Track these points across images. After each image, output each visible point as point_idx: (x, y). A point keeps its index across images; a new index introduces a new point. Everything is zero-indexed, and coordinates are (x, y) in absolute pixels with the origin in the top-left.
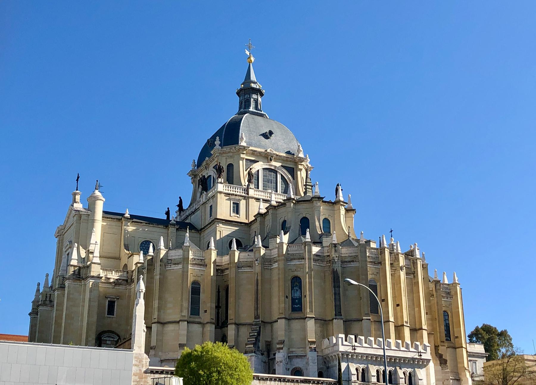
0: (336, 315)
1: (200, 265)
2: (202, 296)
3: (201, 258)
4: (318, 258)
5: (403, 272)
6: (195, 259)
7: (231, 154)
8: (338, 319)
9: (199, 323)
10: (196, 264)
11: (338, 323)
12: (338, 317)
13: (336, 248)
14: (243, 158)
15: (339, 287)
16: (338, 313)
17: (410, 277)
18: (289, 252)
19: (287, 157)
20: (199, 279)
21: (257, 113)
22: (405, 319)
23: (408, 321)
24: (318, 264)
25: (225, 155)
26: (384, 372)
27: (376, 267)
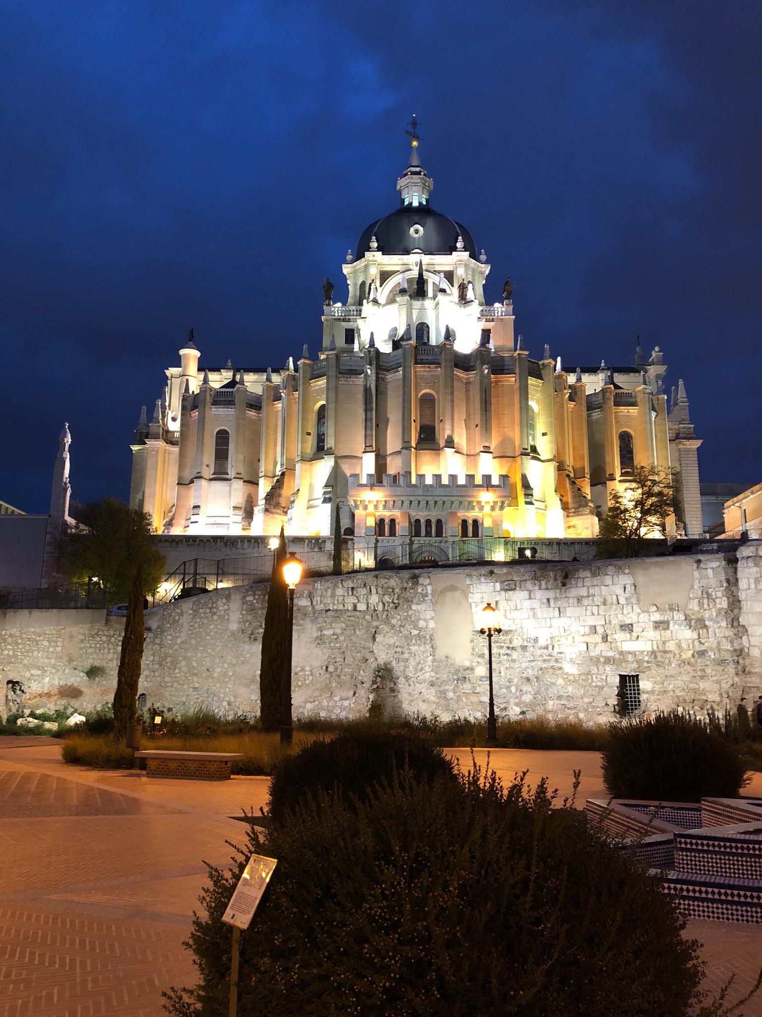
26: (428, 522)
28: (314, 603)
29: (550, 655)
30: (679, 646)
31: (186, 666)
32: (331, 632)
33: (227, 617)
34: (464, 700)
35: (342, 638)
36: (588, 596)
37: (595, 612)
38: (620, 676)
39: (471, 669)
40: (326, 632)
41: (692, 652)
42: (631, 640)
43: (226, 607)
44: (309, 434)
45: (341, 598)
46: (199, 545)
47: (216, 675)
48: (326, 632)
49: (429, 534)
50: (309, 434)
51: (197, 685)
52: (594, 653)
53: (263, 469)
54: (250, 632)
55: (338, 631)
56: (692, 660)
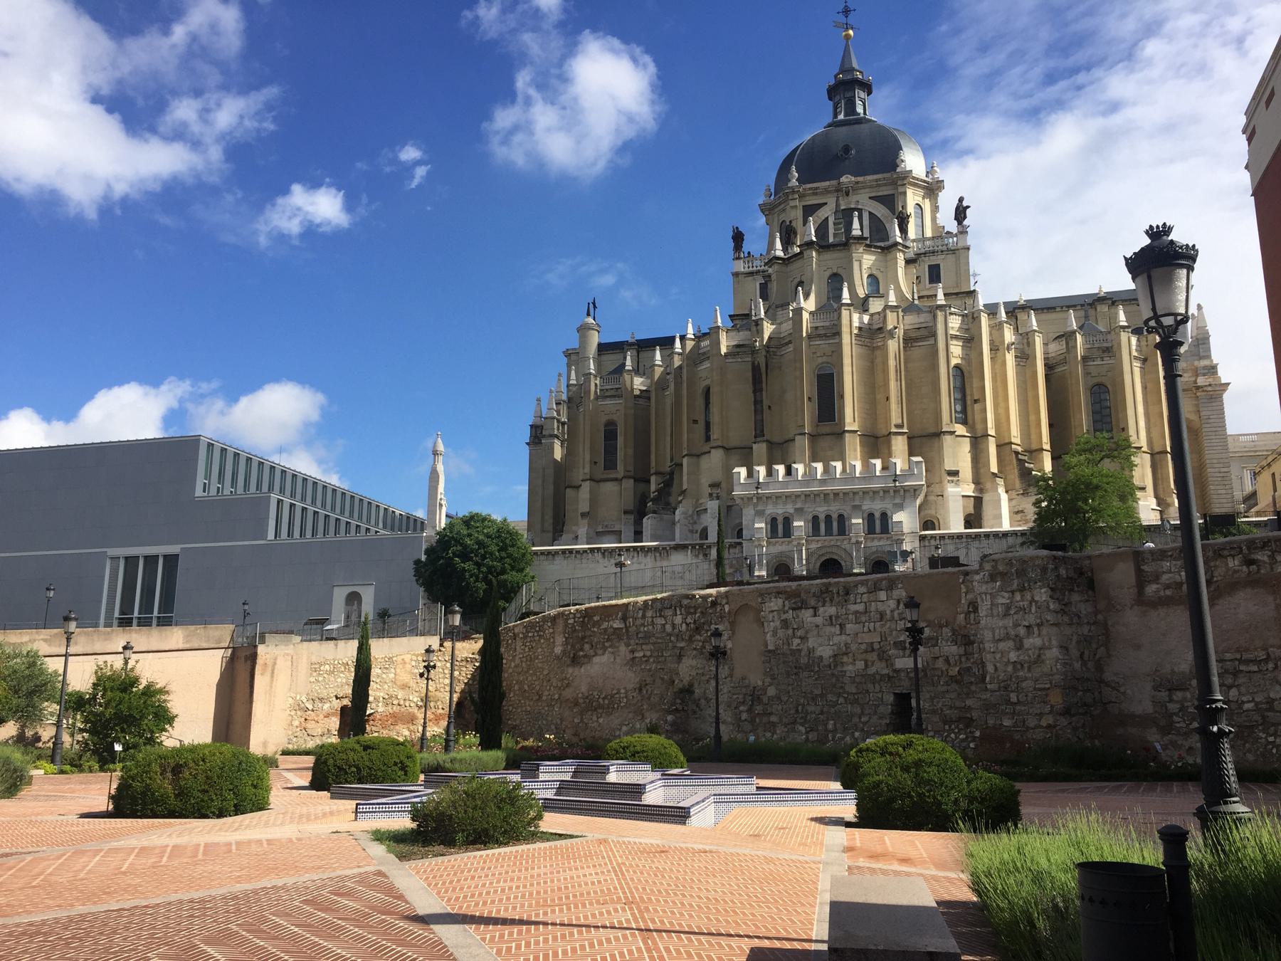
0: (755, 437)
1: (614, 396)
2: (620, 440)
3: (617, 386)
4: (738, 350)
5: (896, 339)
6: (607, 390)
7: (782, 206)
8: (758, 442)
9: (616, 479)
10: (607, 397)
11: (760, 449)
12: (758, 439)
13: (759, 327)
14: (796, 207)
15: (761, 390)
16: (759, 434)
17: (928, 343)
18: (701, 351)
19: (877, 180)
20: (615, 417)
21: (850, 120)
22: (895, 418)
23: (903, 422)
24: (739, 360)
25: (776, 210)
26: (828, 518)
27: (831, 341)
28: (628, 624)
29: (833, 674)
30: (947, 661)
31: (520, 689)
32: (641, 654)
33: (552, 640)
34: (757, 720)
35: (651, 660)
36: (866, 612)
37: (872, 629)
38: (895, 694)
39: (765, 690)
40: (637, 655)
41: (957, 669)
42: (904, 656)
43: (551, 630)
44: (695, 422)
45: (650, 620)
46: (575, 557)
47: (544, 698)
48: (637, 655)
49: (829, 532)
50: (695, 422)
51: (529, 709)
52: (872, 670)
53: (653, 464)
54: (572, 655)
55: (648, 653)
56: (959, 678)
